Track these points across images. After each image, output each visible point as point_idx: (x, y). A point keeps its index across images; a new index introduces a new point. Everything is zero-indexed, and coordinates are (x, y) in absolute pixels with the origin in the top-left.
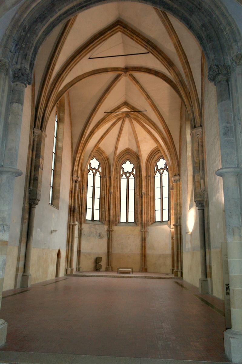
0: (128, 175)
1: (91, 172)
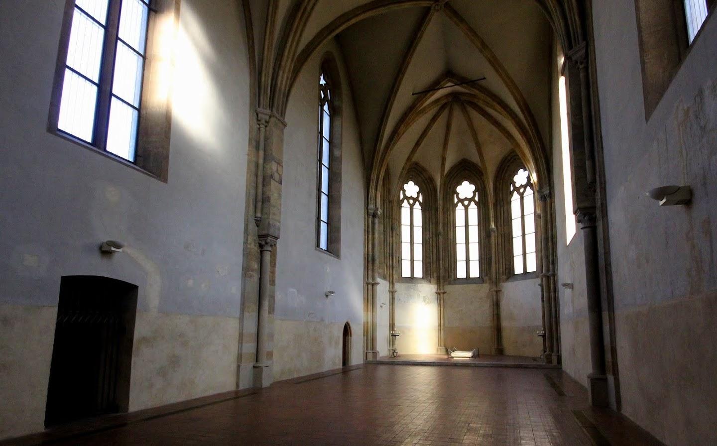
0: (466, 203)
1: (405, 204)
